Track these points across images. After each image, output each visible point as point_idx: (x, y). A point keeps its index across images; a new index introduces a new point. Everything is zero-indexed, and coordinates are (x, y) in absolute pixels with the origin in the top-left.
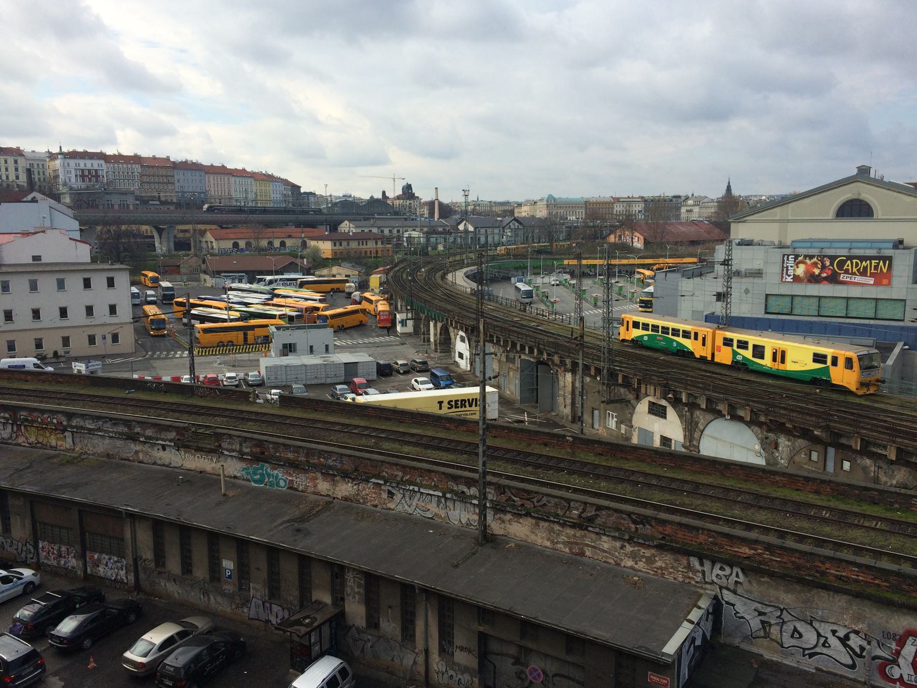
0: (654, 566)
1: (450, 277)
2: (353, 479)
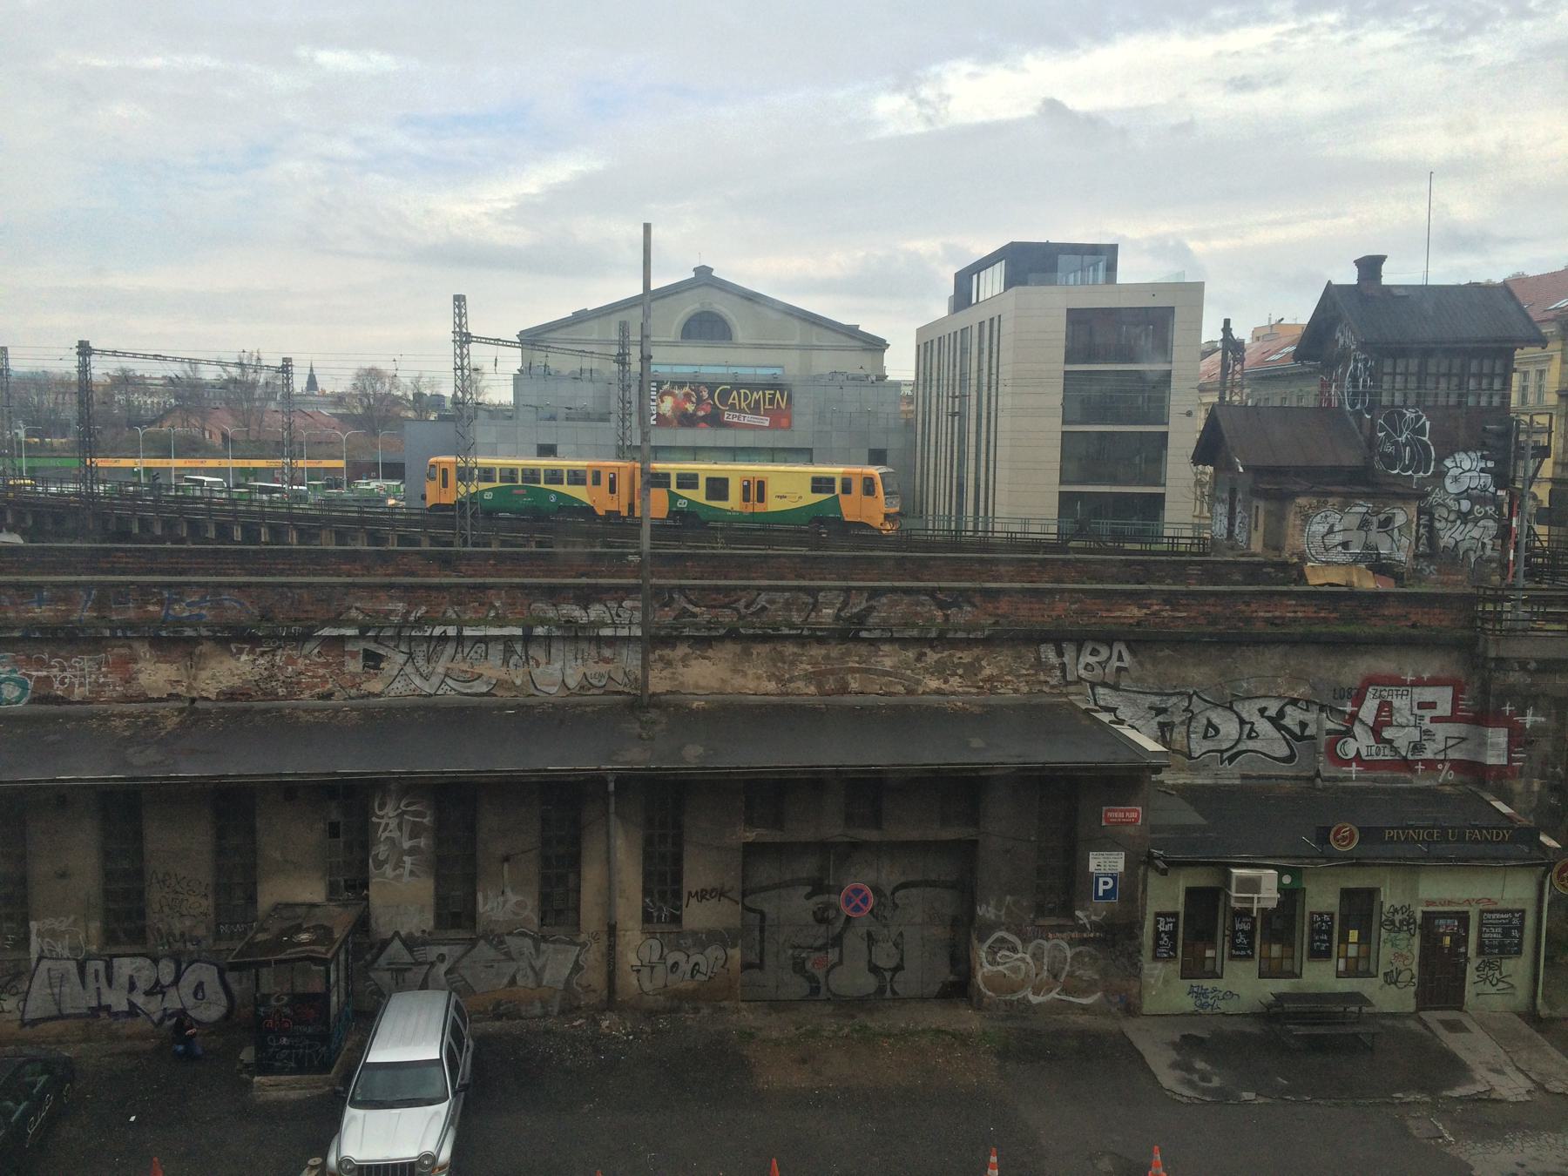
0: (980, 677)
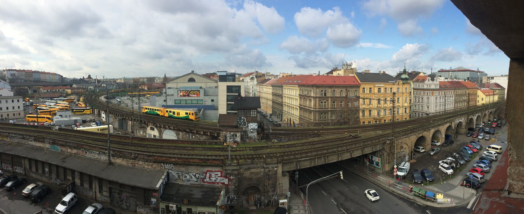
1: (100, 98)
2: (77, 149)
